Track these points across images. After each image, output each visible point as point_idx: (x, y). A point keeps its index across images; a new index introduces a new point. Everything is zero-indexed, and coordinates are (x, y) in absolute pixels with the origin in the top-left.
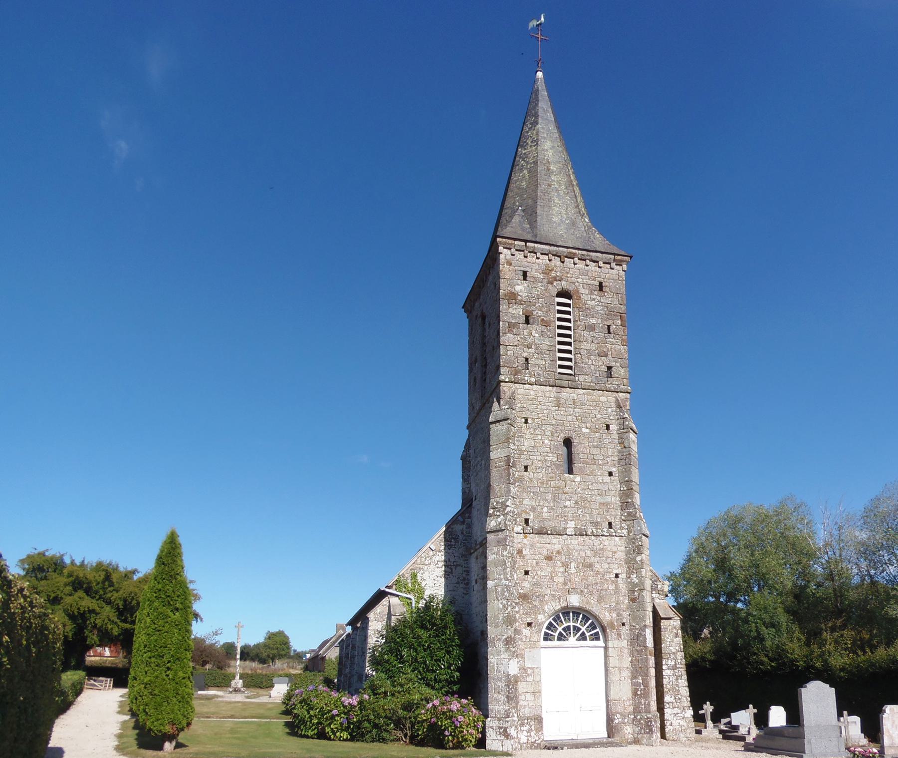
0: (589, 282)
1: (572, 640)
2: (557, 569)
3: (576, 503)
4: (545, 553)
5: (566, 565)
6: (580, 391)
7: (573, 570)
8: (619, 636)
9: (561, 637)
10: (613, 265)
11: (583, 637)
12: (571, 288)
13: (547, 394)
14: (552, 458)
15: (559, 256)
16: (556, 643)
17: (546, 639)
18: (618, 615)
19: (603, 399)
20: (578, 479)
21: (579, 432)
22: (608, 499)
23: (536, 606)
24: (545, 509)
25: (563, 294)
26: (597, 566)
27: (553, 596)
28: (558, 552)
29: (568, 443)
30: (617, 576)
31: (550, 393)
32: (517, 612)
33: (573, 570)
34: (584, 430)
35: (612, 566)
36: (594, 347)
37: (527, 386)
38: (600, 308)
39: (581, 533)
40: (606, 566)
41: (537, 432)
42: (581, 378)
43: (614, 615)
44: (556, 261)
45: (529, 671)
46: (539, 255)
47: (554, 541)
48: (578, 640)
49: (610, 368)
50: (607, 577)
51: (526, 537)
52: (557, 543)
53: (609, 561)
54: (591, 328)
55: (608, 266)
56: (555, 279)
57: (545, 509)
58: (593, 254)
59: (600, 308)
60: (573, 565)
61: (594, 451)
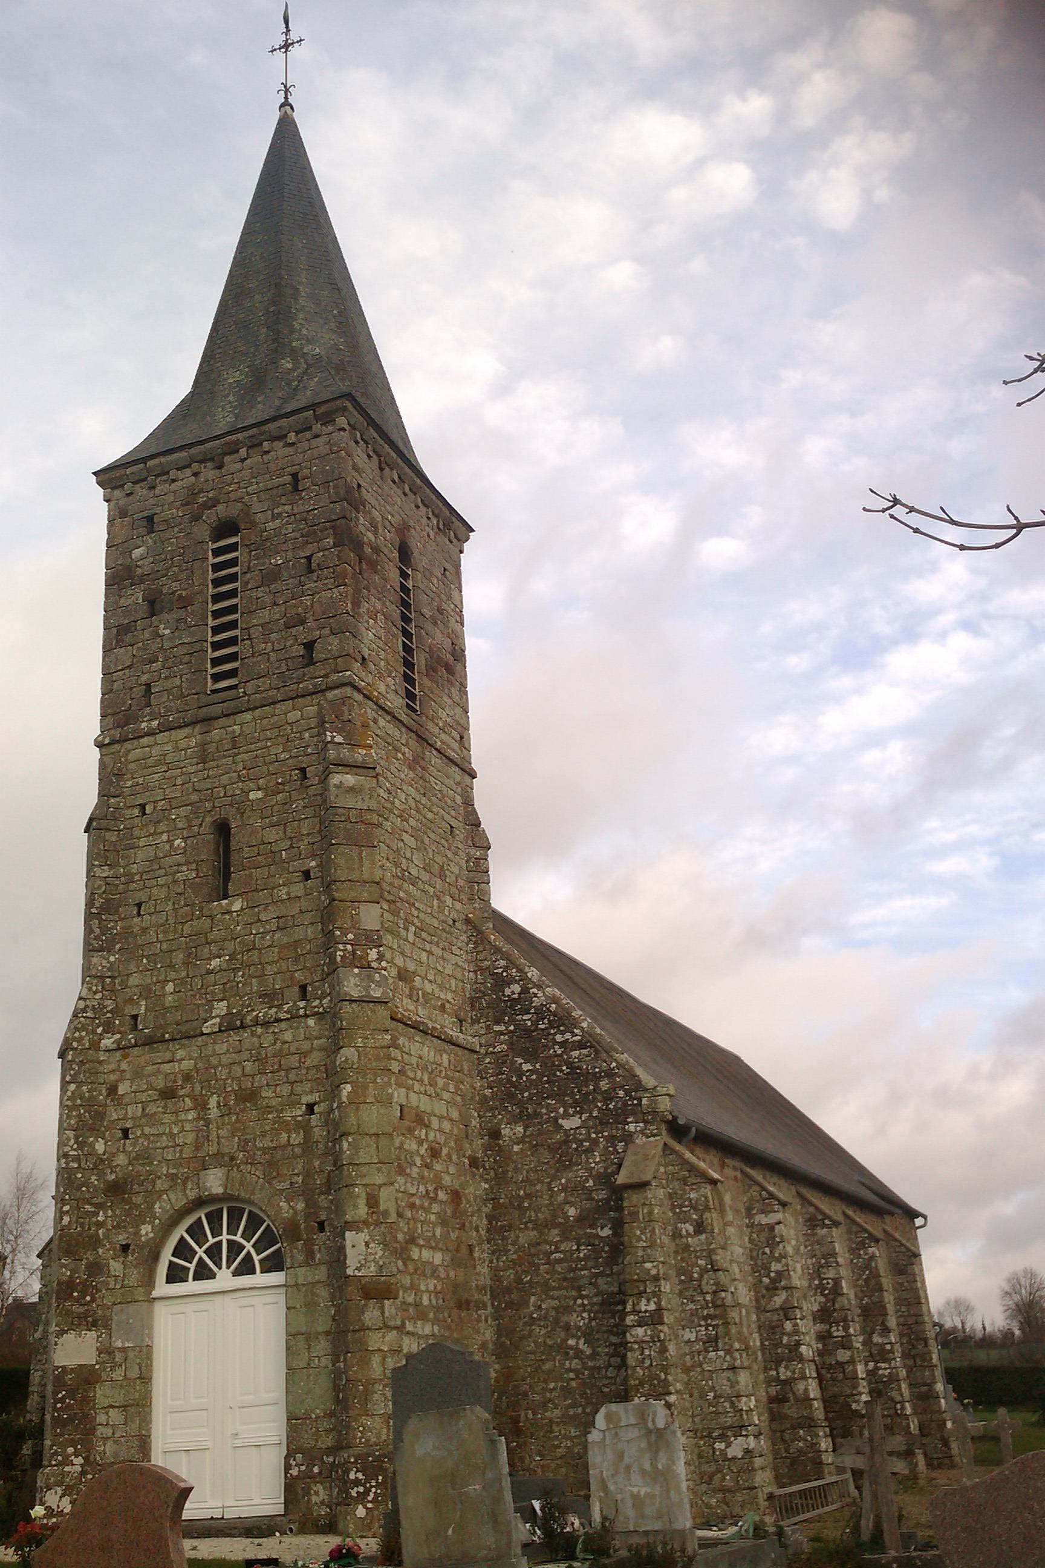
0: (270, 484)
1: (224, 1278)
2: (182, 1116)
3: (232, 956)
4: (160, 1082)
5: (201, 1105)
6: (248, 716)
7: (214, 1113)
8: (310, 1254)
9: (203, 1273)
10: (317, 427)
11: (246, 1268)
12: (234, 511)
13: (183, 744)
14: (187, 873)
15: (212, 459)
16: (191, 1286)
17: (171, 1279)
18: (310, 1203)
19: (293, 716)
20: (237, 905)
21: (242, 805)
22: (299, 933)
23: (138, 1206)
24: (170, 987)
25: (226, 528)
26: (267, 1093)
27: (173, 1177)
28: (187, 1078)
29: (223, 829)
30: (310, 1108)
31: (188, 739)
32: (100, 1225)
33: (214, 1113)
34: (252, 796)
35: (298, 1089)
36: (277, 613)
37: (145, 741)
38: (290, 528)
39: (231, 1025)
40: (285, 1090)
41: (162, 827)
42: (250, 687)
43: (300, 1206)
44: (209, 473)
45: (119, 1357)
46: (173, 474)
47: (181, 1053)
48: (237, 1273)
49: (309, 646)
50: (287, 1115)
51: (125, 1057)
52: (184, 1059)
53: (292, 1076)
54: (271, 577)
55: (308, 435)
56: (206, 506)
57: (170, 987)
58: (271, 426)
59: (290, 528)
60: (213, 1101)
61: (272, 835)
